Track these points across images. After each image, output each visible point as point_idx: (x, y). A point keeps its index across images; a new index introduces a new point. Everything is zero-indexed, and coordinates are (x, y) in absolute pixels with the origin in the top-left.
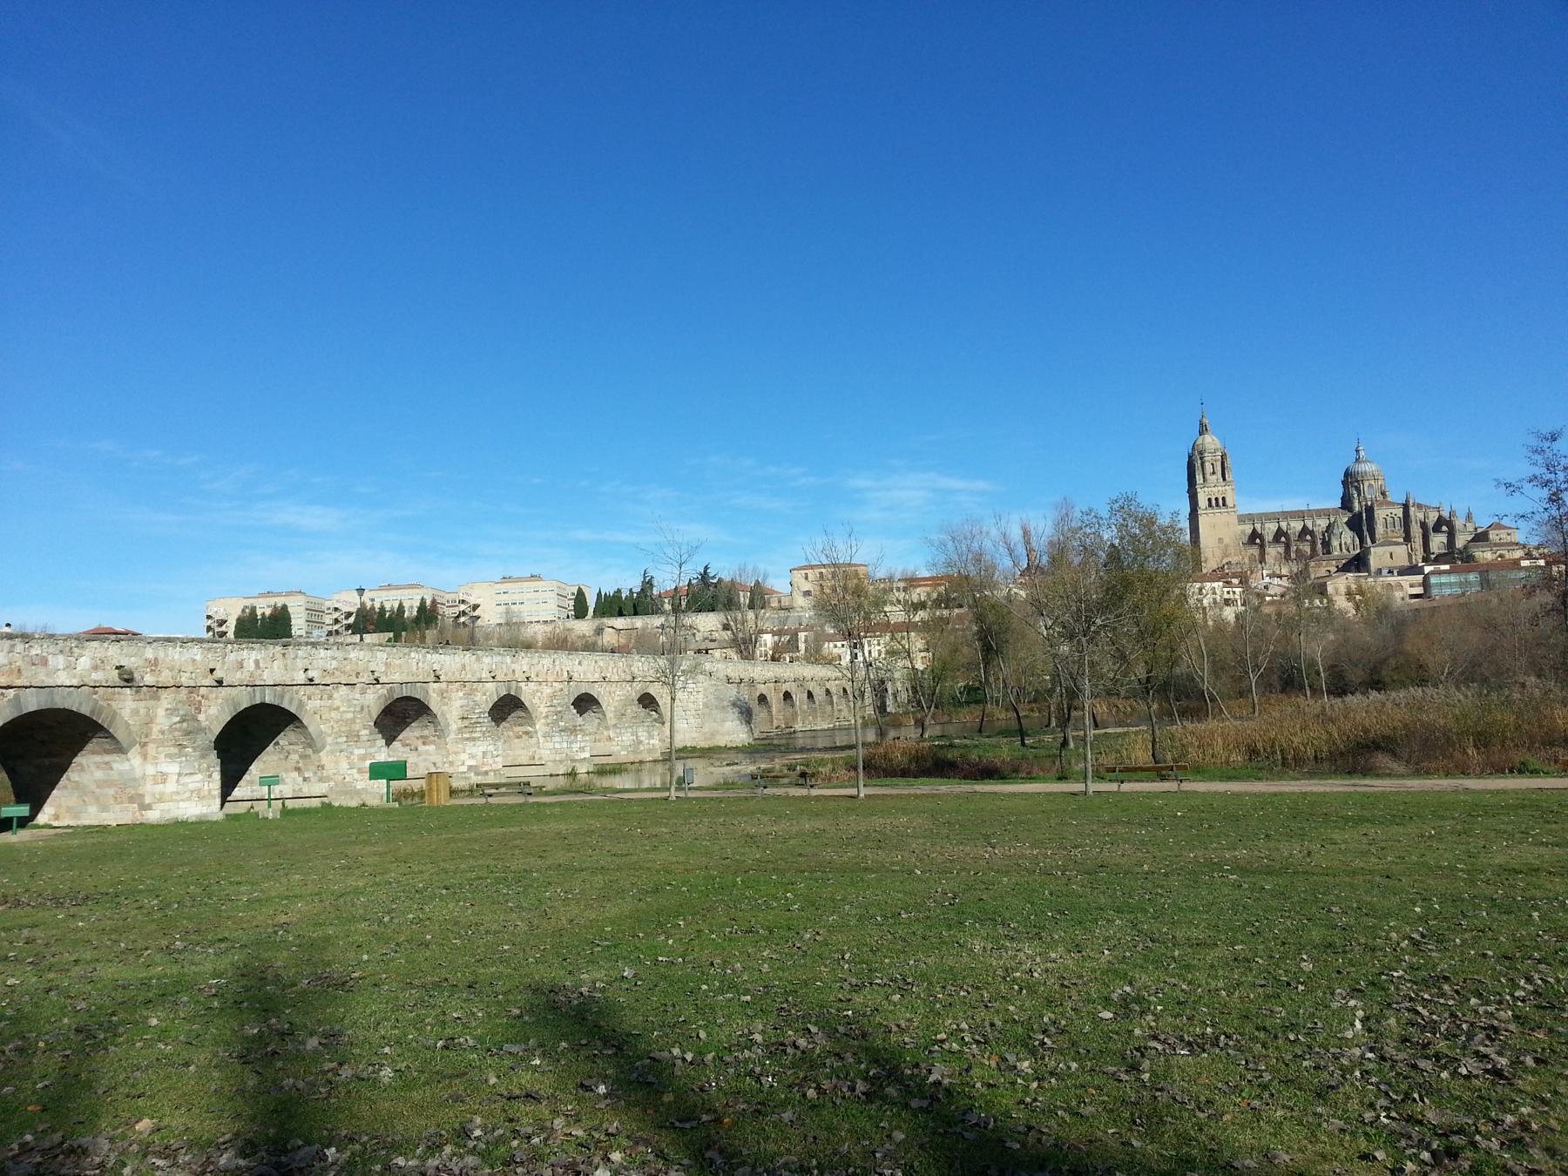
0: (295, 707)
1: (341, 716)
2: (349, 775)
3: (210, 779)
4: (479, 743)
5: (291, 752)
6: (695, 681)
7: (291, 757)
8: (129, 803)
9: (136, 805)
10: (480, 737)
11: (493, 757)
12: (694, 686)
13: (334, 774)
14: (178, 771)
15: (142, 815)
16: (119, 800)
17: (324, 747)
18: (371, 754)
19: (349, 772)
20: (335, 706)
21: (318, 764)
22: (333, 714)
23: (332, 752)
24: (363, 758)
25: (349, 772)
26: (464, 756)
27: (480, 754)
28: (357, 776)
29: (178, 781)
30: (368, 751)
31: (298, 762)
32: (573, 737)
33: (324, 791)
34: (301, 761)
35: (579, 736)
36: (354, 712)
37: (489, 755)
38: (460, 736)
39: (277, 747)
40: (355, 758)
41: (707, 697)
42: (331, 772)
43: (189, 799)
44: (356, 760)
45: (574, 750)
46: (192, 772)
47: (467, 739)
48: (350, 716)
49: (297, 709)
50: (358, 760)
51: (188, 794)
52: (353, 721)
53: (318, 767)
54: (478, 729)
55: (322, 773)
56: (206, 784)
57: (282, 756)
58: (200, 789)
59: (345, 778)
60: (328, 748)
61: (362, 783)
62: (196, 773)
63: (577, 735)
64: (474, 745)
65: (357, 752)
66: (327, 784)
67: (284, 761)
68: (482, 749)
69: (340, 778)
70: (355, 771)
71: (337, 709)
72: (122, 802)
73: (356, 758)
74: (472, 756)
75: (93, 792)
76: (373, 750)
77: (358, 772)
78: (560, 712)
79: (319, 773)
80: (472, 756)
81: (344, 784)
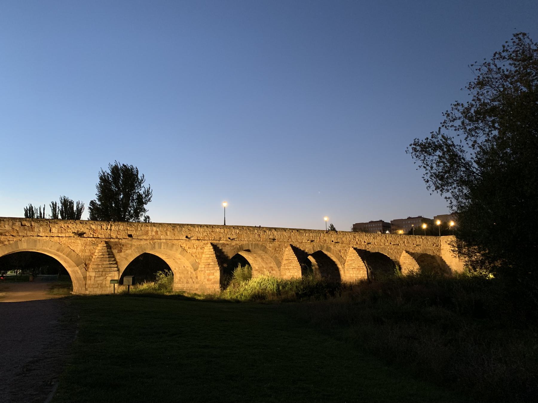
3: (105, 280)
10: (291, 269)
18: (212, 273)
24: (209, 275)
28: (207, 282)
29: (94, 280)
30: (211, 271)
43: (97, 287)
48: (208, 256)
51: (97, 285)
54: (291, 265)
58: (102, 283)
62: (100, 277)
65: (207, 272)
76: (213, 271)
78: (353, 260)
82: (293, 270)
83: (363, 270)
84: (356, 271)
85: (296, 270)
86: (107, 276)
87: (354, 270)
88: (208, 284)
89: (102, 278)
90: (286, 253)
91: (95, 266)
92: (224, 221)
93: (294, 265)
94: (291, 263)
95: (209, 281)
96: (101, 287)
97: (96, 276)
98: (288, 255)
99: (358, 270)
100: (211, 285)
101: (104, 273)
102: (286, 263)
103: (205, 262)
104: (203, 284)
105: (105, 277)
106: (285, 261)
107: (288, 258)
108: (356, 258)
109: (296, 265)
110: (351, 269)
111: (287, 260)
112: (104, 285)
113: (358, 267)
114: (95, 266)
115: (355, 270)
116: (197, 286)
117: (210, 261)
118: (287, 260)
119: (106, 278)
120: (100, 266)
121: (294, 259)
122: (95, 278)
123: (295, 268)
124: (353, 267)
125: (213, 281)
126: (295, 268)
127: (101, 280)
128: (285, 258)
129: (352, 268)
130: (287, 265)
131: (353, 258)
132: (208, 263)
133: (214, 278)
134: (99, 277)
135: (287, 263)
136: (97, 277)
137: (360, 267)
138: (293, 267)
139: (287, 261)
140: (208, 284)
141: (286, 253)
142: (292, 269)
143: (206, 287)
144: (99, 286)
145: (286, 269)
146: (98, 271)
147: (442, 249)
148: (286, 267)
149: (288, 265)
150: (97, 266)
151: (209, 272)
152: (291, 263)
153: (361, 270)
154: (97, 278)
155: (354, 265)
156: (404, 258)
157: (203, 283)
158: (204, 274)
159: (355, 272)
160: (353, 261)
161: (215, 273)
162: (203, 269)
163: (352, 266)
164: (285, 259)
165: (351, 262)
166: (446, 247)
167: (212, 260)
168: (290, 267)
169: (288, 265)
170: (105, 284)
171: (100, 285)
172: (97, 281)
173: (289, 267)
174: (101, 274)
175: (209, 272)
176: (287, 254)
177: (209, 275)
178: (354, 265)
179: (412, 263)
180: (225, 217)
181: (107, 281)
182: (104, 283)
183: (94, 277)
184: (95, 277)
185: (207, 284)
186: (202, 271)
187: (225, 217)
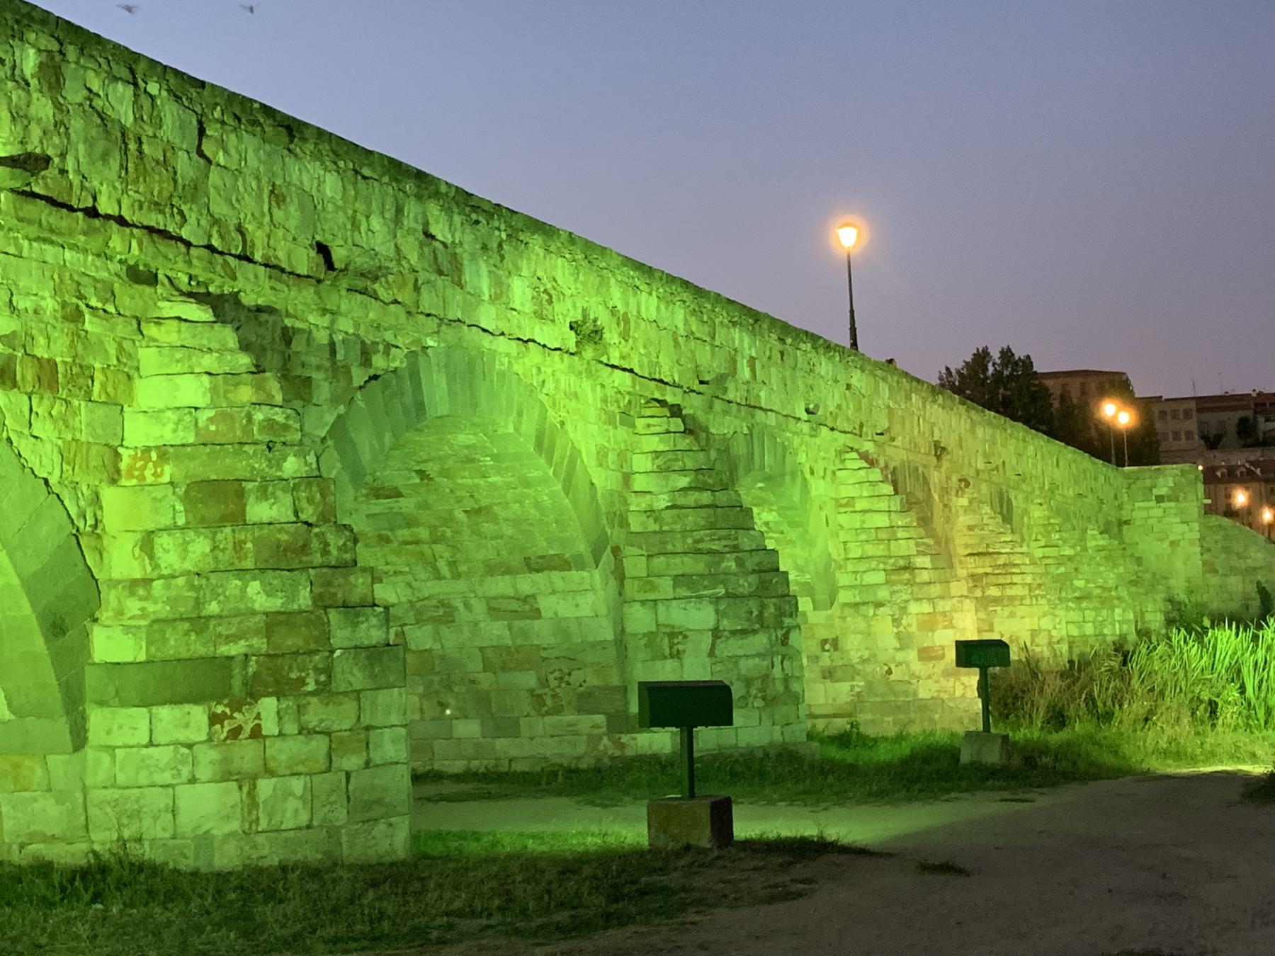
2: (899, 664)
3: (783, 650)
4: (1021, 610)
8: (580, 711)
9: (600, 719)
10: (1022, 598)
13: (864, 661)
14: (711, 624)
15: (623, 746)
16: (549, 702)
18: (944, 614)
19: (900, 656)
25: (900, 656)
28: (917, 667)
29: (711, 653)
35: (1118, 611)
40: (911, 623)
41: (1209, 550)
42: (854, 657)
44: (913, 629)
46: (746, 625)
47: (997, 601)
48: (882, 521)
53: (825, 641)
54: (1016, 579)
56: (777, 660)
59: (890, 672)
62: (754, 632)
64: (1012, 615)
65: (914, 608)
68: (1029, 624)
69: (880, 670)
70: (912, 655)
72: (558, 710)
75: (473, 682)
77: (920, 659)
78: (1070, 558)
81: (888, 683)
82: (1031, 605)
83: (1124, 605)
84: (1095, 609)
85: (1043, 601)
86: (789, 629)
87: (1084, 605)
88: (930, 677)
89: (760, 641)
90: (961, 519)
91: (690, 565)
92: (848, 332)
93: (1029, 579)
94: (1014, 570)
95: (930, 659)
96: (764, 699)
97: (726, 624)
98: (977, 531)
99: (1103, 603)
100: (943, 681)
101: (772, 609)
102: (981, 571)
103: (880, 553)
104: (892, 677)
105: (780, 633)
106: (971, 559)
107: (988, 546)
108: (1079, 548)
109: (1039, 581)
110: (1069, 600)
111: (979, 554)
112: (780, 687)
113: (1099, 591)
114: (690, 565)
115: (1091, 606)
116: (842, 692)
117: (904, 547)
118: (979, 554)
119: (785, 641)
120: (730, 564)
121: (1018, 550)
122: (720, 645)
123: (1037, 592)
124: (1077, 594)
126: (1042, 597)
127: (759, 655)
128: (967, 546)
129: (1078, 598)
130: (992, 579)
131: (1068, 552)
132: (902, 563)
134: (743, 632)
135: (989, 570)
136: (733, 633)
137: (1110, 590)
138: (1030, 591)
139: (988, 560)
140: (930, 677)
141: (963, 520)
142: (1027, 601)
143: (915, 693)
144: (753, 691)
145: (997, 601)
146: (729, 595)
147: (1127, 522)
148: (994, 592)
149: (1001, 580)
150: (709, 565)
151: (926, 608)
152: (1014, 570)
153: (1115, 602)
154: (732, 641)
155: (1079, 583)
156: (1103, 554)
157: (893, 667)
158: (896, 621)
159: (1090, 615)
160: (1070, 565)
161: (955, 615)
162: (883, 594)
163: (1075, 589)
164: (970, 551)
165: (1062, 569)
166: (1144, 514)
167: (917, 545)
168: (1015, 587)
169: (1001, 580)
170: (786, 680)
171: (758, 684)
172: (735, 659)
173: (1010, 592)
174: (755, 613)
175: (926, 608)
176: (971, 528)
177: (929, 624)
178: (1079, 583)
179: (1140, 575)
180: (852, 312)
181: (791, 658)
182: (777, 672)
183: (707, 639)
184: (716, 633)
185: (919, 678)
186: (879, 605)
187: (852, 312)
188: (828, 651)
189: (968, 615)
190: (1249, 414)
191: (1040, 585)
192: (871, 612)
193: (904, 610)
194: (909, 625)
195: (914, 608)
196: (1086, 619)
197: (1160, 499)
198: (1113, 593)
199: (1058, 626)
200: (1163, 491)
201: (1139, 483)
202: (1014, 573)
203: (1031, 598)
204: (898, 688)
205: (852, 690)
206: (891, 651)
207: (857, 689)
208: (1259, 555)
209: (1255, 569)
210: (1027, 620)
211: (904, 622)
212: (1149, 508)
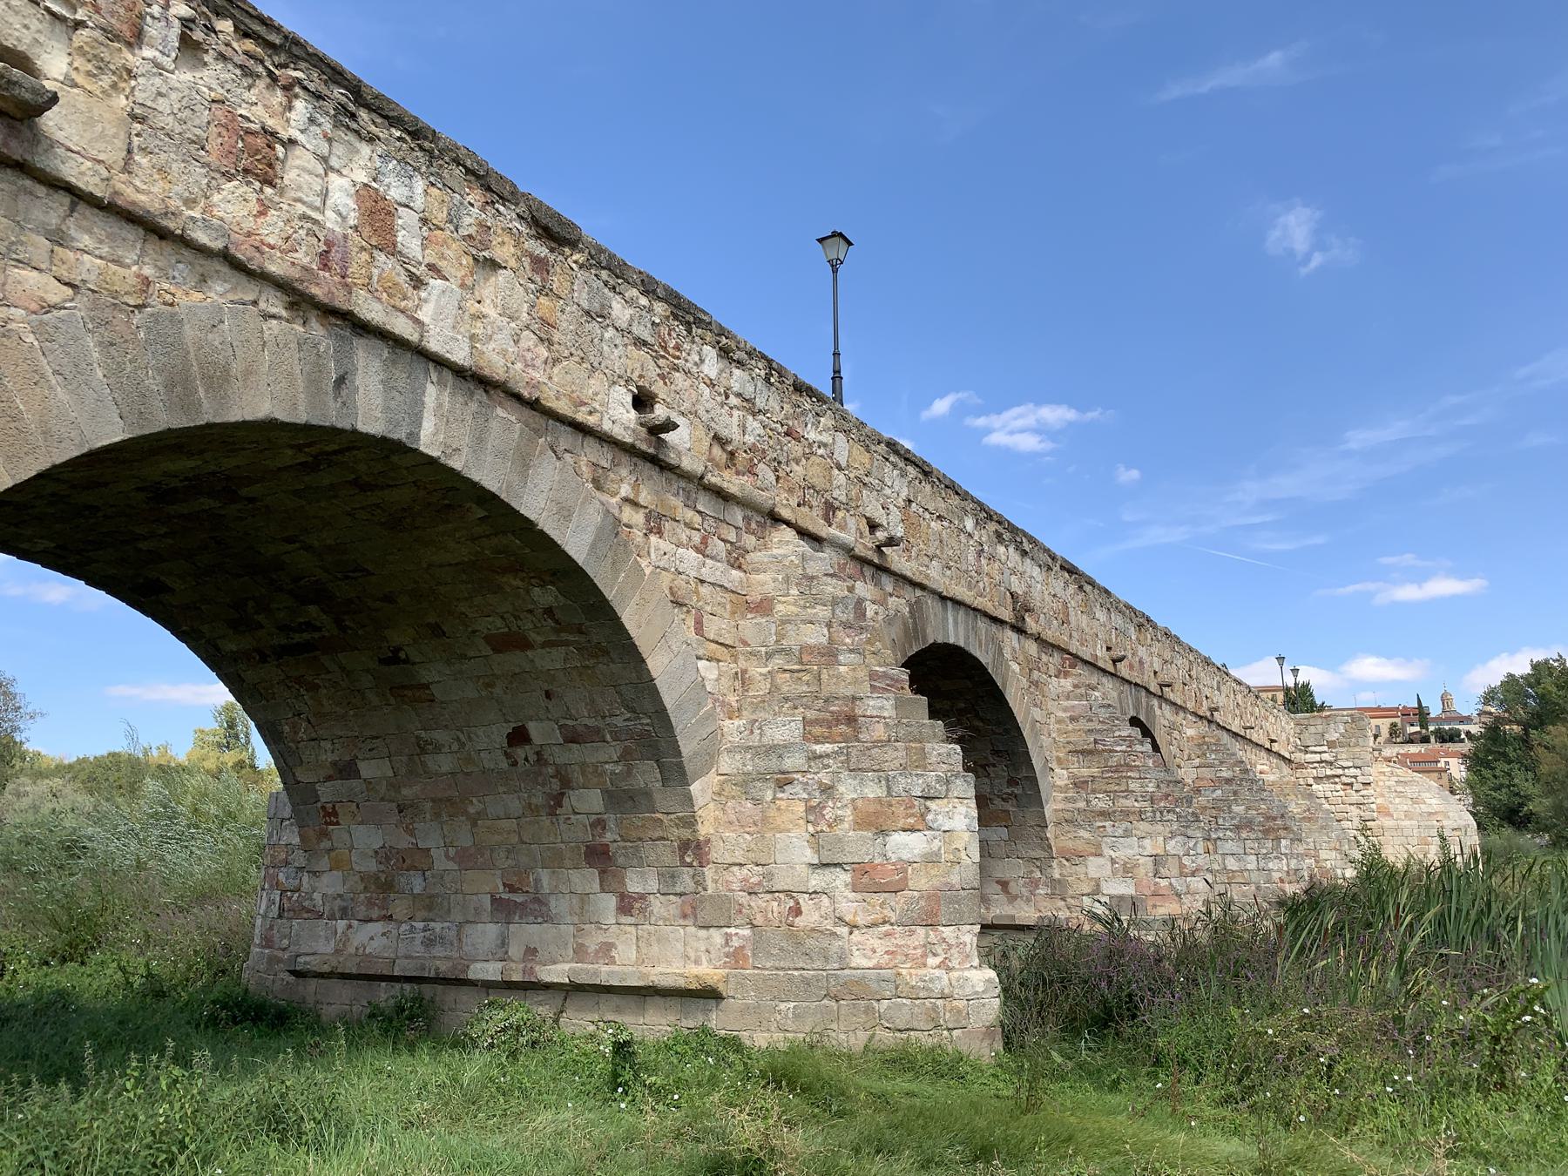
0: (588, 537)
1: (781, 636)
5: (577, 777)
6: (1359, 763)
7: (574, 799)
11: (1182, 874)
12: (1357, 772)
17: (709, 758)
19: (817, 881)
20: (755, 597)
21: (686, 834)
22: (750, 626)
23: (745, 784)
26: (1096, 867)
27: (1146, 865)
28: (849, 904)
31: (600, 824)
32: (1269, 844)
33: (706, 971)
34: (611, 819)
35: (1283, 842)
36: (829, 625)
37: (1171, 869)
38: (1082, 805)
39: (520, 752)
45: (1276, 876)
47: (1104, 814)
48: (815, 636)
49: (593, 546)
50: (859, 824)
52: (829, 654)
55: (700, 882)
57: (538, 800)
59: (797, 911)
60: (727, 764)
61: (872, 940)
63: (1278, 839)
64: (1127, 834)
65: (847, 789)
66: (717, 936)
67: (546, 821)
68: (1150, 846)
69: (776, 908)
71: (763, 607)
73: (848, 813)
74: (1128, 870)
78: (1228, 781)
79: (686, 881)
80: (1128, 870)
83: (1292, 836)
104: (800, 922)
115: (1253, 836)
125: (921, 882)
133: (931, 859)
137: (1274, 819)
143: (842, 957)
145: (1104, 814)
153: (1282, 833)
155: (1239, 809)
158: (813, 811)
162: (793, 761)
175: (873, 791)
177: (876, 822)
178: (1239, 809)
185: (853, 927)
188: (690, 865)
189: (962, 809)
190: (1397, 720)
191: (1167, 796)
192: (769, 795)
193: (827, 790)
194: (838, 820)
195: (847, 789)
196: (1248, 850)
197: (1331, 745)
198: (1279, 822)
199: (1192, 852)
200: (1333, 736)
201: (1312, 729)
202: (1130, 777)
203: (1153, 812)
204: (810, 943)
205: (727, 943)
206: (802, 870)
207: (736, 943)
208: (1434, 801)
209: (1430, 814)
210: (1147, 842)
211: (828, 813)
212: (1320, 753)
